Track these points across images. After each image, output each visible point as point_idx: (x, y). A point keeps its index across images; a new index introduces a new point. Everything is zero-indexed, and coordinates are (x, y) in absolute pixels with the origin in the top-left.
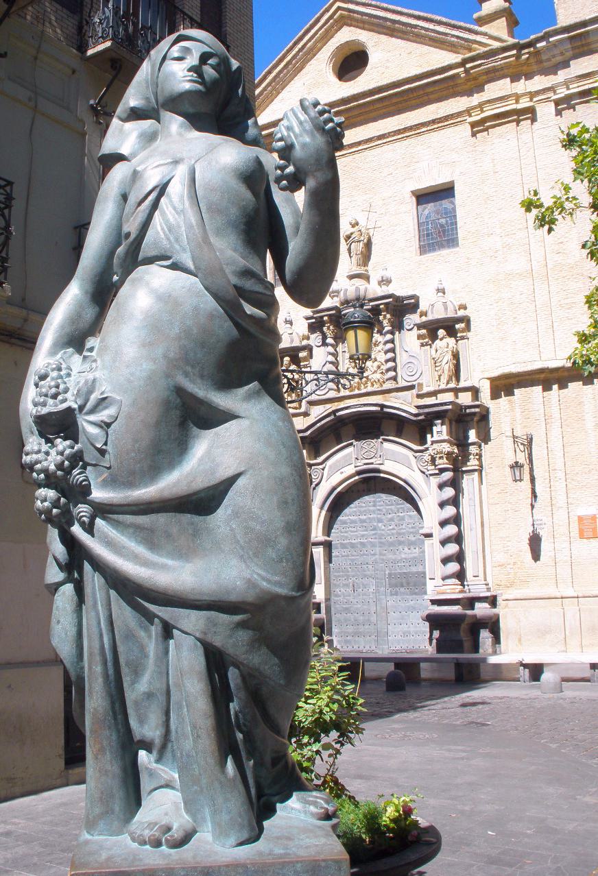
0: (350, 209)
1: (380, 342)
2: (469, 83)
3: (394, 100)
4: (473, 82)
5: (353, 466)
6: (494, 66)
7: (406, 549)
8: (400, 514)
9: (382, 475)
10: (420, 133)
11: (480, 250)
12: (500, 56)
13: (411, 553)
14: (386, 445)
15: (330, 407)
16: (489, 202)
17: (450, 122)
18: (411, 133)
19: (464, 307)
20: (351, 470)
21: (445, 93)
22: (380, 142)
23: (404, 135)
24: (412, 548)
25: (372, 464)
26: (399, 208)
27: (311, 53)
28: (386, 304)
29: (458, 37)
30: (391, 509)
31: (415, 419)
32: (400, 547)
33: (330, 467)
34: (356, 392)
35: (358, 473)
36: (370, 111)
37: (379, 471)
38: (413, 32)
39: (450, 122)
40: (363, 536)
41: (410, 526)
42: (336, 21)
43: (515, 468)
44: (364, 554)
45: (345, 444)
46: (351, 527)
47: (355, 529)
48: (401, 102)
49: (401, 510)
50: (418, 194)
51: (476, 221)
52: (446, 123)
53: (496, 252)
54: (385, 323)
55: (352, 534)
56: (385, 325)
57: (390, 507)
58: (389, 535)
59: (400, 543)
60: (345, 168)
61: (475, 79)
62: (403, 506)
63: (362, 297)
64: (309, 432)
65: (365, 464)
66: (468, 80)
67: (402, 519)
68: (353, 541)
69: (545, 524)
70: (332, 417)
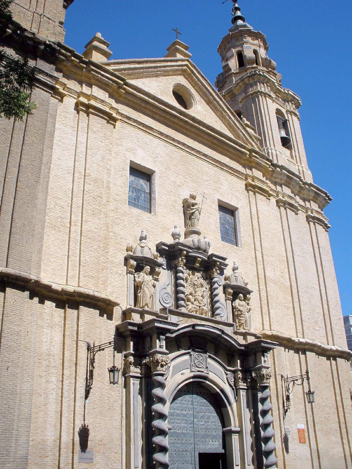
2: (246, 162)
3: (215, 141)
4: (248, 162)
5: (189, 370)
6: (261, 163)
7: (211, 441)
8: (207, 414)
9: (207, 382)
10: (223, 169)
12: (265, 161)
13: (214, 445)
14: (210, 361)
17: (236, 174)
18: (219, 166)
21: (234, 157)
22: (203, 157)
23: (216, 164)
24: (214, 441)
25: (202, 372)
27: (166, 74)
29: (244, 135)
30: (202, 409)
31: (239, 348)
32: (207, 440)
33: (174, 367)
34: (192, 314)
35: (194, 377)
36: (200, 136)
37: (206, 378)
38: (221, 113)
39: (236, 174)
40: (184, 427)
41: (213, 424)
42: (182, 70)
43: (310, 394)
44: (185, 443)
46: (176, 419)
47: (179, 421)
48: (215, 144)
49: (208, 411)
50: (222, 205)
52: (235, 174)
55: (177, 425)
57: (202, 407)
58: (201, 429)
59: (208, 436)
60: (182, 158)
61: (250, 162)
62: (209, 408)
65: (198, 371)
66: (248, 160)
67: (209, 417)
68: (178, 431)
69: (290, 432)
70: (190, 329)
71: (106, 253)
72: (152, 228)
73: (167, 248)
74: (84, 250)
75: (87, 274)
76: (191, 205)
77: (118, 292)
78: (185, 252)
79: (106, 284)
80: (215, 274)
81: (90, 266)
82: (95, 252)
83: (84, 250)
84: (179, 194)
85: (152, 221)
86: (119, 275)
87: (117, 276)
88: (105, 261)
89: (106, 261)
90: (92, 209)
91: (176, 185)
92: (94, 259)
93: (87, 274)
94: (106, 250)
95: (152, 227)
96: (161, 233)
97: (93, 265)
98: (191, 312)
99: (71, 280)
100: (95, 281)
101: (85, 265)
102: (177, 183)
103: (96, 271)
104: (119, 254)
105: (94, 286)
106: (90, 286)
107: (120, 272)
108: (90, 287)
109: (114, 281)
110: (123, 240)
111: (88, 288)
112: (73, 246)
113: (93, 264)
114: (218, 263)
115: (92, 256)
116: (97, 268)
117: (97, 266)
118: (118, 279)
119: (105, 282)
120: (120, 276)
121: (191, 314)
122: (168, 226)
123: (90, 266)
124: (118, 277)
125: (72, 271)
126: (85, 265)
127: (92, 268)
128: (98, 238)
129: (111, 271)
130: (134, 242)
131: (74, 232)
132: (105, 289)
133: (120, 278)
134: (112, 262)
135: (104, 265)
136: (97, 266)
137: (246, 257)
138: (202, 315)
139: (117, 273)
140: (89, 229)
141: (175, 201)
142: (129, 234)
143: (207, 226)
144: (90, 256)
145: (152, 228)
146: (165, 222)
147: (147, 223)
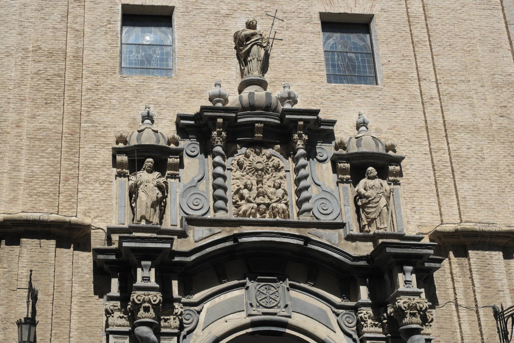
0: (239, 11)
1: (283, 167)
11: (408, 93)
15: (224, 232)
16: (419, 46)
19: (392, 148)
20: (241, 319)
26: (305, 26)
28: (306, 121)
45: (236, 282)
51: (403, 62)
53: (432, 98)
54: (300, 143)
56: (297, 147)
63: (273, 107)
64: (193, 257)
71: (72, 154)
72: (166, 98)
73: (193, 122)
74: (30, 159)
75: (35, 191)
76: (245, 39)
77: (99, 208)
78: (301, 123)
79: (73, 200)
80: (298, 143)
81: (41, 179)
82: (49, 158)
83: (30, 159)
84: (226, 28)
85: (167, 86)
86: (102, 183)
87: (97, 185)
88: (71, 167)
89: (73, 167)
90: (43, 97)
91: (220, 15)
92: (48, 168)
93: (35, 191)
94: (74, 151)
95: (166, 96)
96: (187, 102)
97: (46, 177)
98: (249, 217)
99: (10, 205)
100: (50, 200)
101: (31, 179)
102: (222, 12)
103: (50, 184)
104: (102, 152)
105: (47, 206)
106: (41, 208)
107: (103, 178)
108: (41, 210)
109: (92, 193)
110: (109, 129)
111: (37, 211)
112: (14, 157)
113: (45, 175)
114: (301, 123)
115: (45, 164)
116: (52, 180)
117: (54, 177)
118: (101, 188)
119: (70, 198)
120: (104, 184)
121: (247, 219)
122: (201, 86)
123: (41, 179)
124: (99, 186)
125: (12, 192)
126: (31, 179)
127: (45, 180)
128: (56, 136)
129: (87, 180)
130: (130, 127)
131: (15, 137)
132: (71, 208)
133: (104, 186)
134: (89, 166)
135: (69, 172)
136: (54, 177)
137: (394, 99)
138: (275, 217)
139: (97, 180)
140: (38, 127)
141: (217, 44)
142: (120, 117)
143: (292, 66)
144: (41, 164)
145: (166, 98)
146: (195, 82)
147: (158, 93)
